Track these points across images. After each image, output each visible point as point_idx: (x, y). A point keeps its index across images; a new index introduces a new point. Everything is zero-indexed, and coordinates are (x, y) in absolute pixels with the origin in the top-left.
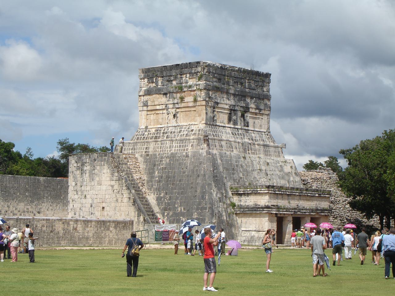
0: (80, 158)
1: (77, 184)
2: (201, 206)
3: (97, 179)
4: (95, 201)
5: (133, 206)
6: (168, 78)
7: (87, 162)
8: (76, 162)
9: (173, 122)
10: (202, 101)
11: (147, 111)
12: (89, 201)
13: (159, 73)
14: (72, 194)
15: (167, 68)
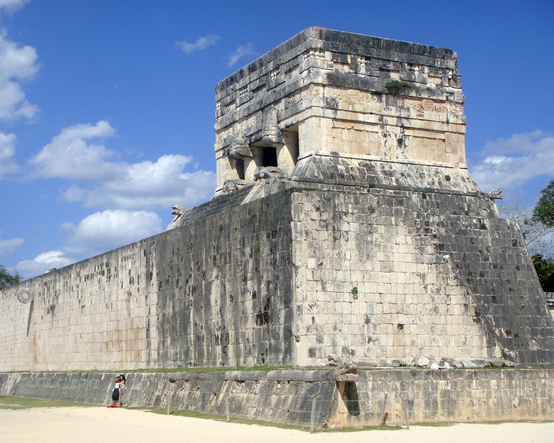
0: (329, 200)
1: (322, 264)
2: (541, 328)
3: (380, 256)
4: (378, 309)
5: (475, 324)
6: (381, 63)
7: (350, 211)
8: (318, 209)
9: (397, 154)
10: (461, 126)
11: (335, 119)
12: (360, 307)
13: (361, 49)
14: (310, 290)
15: (379, 44)
